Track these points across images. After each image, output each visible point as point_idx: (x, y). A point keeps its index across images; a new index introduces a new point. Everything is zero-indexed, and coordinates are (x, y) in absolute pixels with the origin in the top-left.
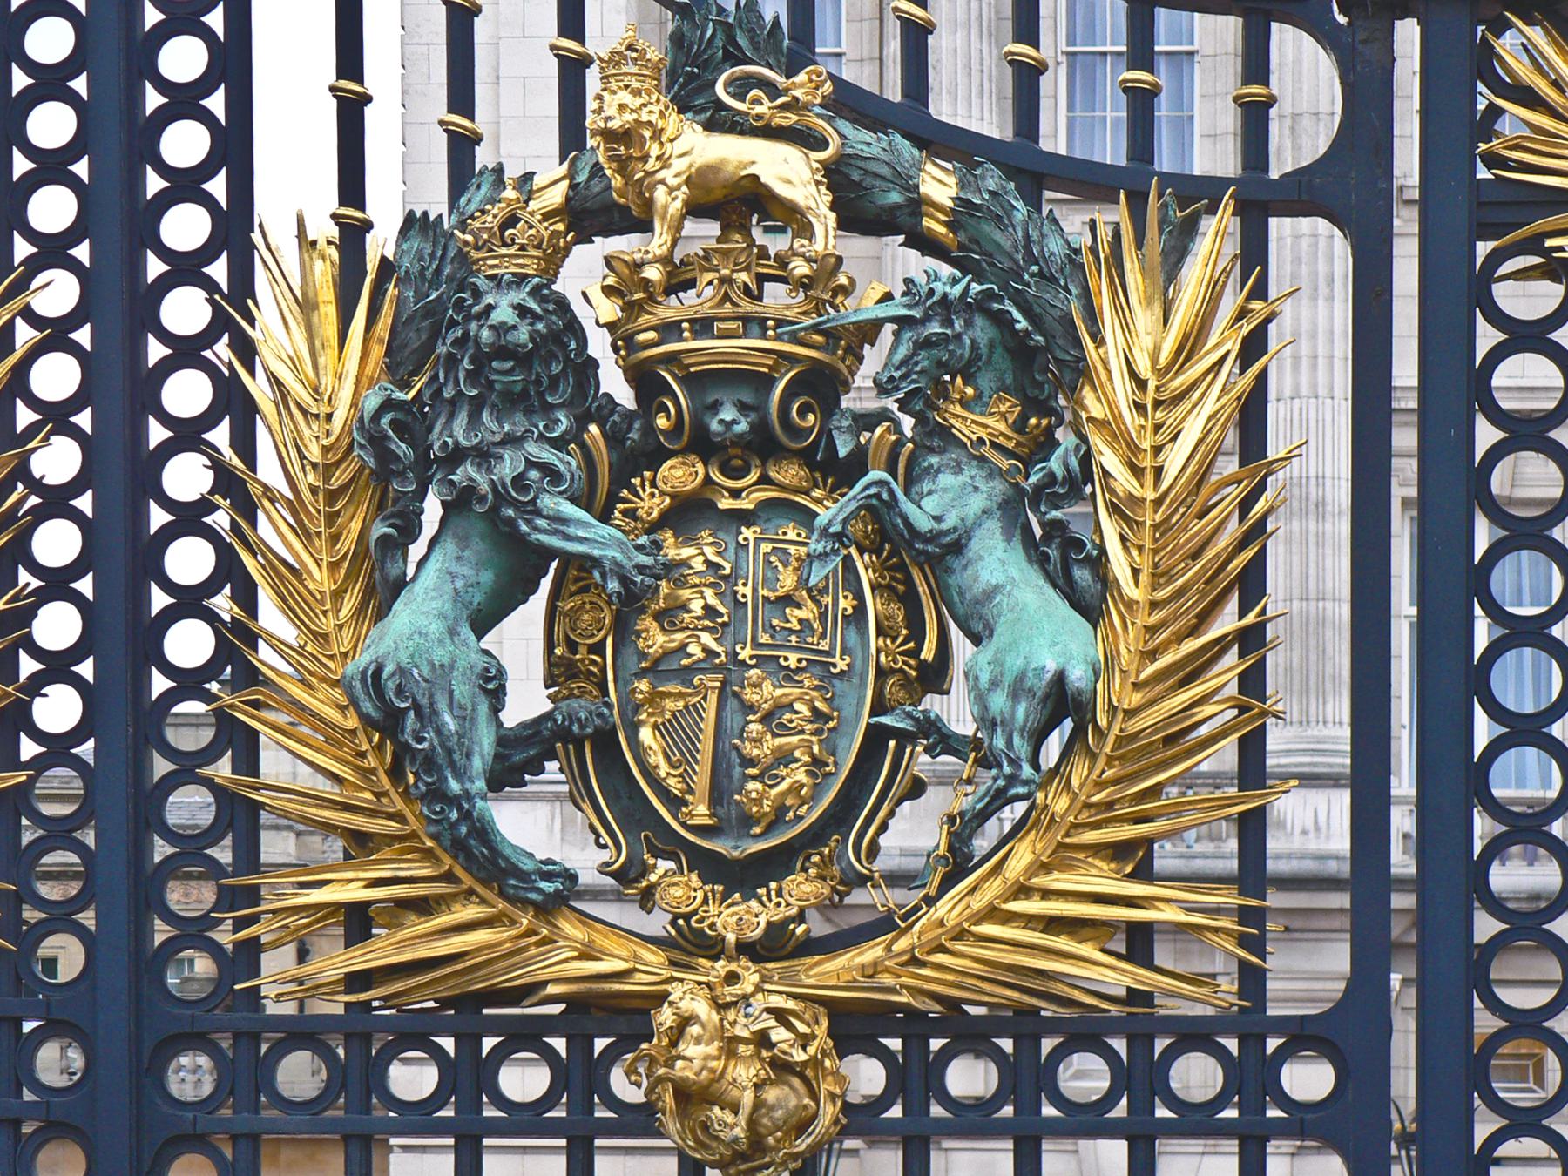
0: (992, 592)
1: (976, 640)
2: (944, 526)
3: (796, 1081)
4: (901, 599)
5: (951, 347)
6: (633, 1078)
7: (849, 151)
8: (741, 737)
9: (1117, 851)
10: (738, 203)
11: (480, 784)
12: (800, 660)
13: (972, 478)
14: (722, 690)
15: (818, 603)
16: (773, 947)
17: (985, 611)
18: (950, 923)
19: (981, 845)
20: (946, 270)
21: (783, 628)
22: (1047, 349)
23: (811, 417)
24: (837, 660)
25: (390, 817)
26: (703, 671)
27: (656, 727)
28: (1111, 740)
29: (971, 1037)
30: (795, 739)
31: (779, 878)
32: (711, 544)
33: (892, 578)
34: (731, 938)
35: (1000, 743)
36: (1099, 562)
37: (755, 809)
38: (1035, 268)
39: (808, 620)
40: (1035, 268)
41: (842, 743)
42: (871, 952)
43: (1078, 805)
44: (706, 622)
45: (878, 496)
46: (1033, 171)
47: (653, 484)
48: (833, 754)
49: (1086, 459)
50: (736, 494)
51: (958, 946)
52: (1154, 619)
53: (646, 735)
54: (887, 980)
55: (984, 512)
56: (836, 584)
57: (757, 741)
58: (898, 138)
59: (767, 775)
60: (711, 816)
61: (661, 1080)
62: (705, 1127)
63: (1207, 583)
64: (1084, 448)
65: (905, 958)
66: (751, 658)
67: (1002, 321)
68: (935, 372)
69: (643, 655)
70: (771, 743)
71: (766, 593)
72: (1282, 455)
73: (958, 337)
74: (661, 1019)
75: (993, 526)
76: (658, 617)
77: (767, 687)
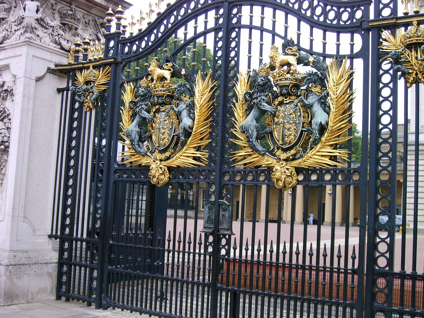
0: (316, 111)
9: (331, 145)
11: (254, 140)
42: (300, 160)
46: (325, 56)
50: (286, 101)
51: (310, 159)
53: (275, 132)
54: (302, 164)
57: (287, 133)
70: (288, 133)
75: (317, 103)
76: (277, 117)
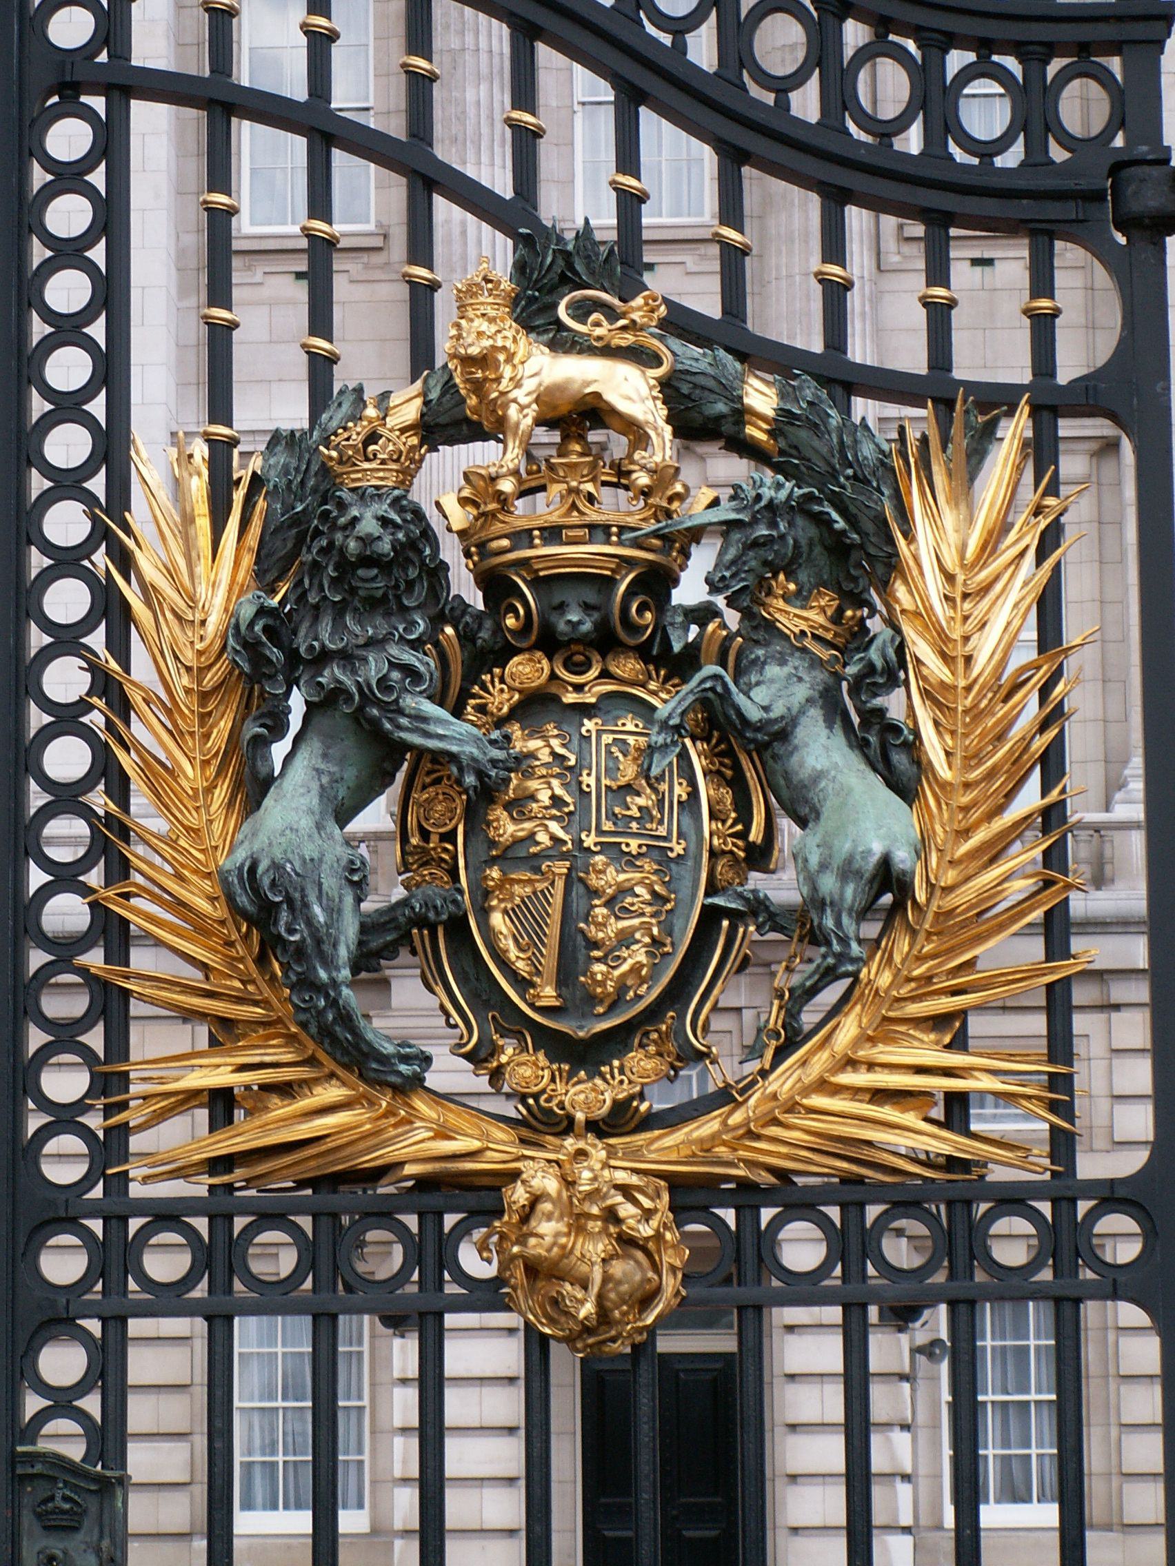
0: (818, 776)
1: (803, 823)
2: (772, 715)
3: (639, 1255)
4: (729, 783)
5: (776, 548)
6: (485, 1255)
7: (680, 367)
8: (586, 922)
10: (580, 416)
12: (640, 846)
13: (796, 668)
14: (568, 876)
15: (655, 790)
16: (618, 1121)
17: (811, 795)
18: (783, 1097)
19: (809, 1018)
20: (768, 476)
21: (624, 816)
22: (861, 547)
23: (648, 615)
24: (673, 844)
25: (256, 1003)
26: (549, 857)
27: (505, 912)
28: (930, 916)
29: (801, 1205)
30: (636, 922)
31: (621, 1054)
32: (556, 736)
33: (721, 764)
34: (580, 1116)
35: (829, 922)
36: (914, 746)
37: (599, 990)
38: (850, 472)
39: (647, 808)
40: (850, 472)
41: (678, 924)
42: (708, 1126)
43: (900, 979)
44: (554, 812)
45: (712, 689)
47: (502, 681)
48: (670, 935)
49: (901, 649)
50: (579, 688)
52: (965, 800)
53: (497, 920)
55: (807, 701)
56: (671, 772)
58: (721, 353)
60: (559, 996)
61: (514, 1258)
62: (555, 1302)
63: (1013, 764)
64: (898, 640)
65: (741, 1132)
66: (596, 844)
67: (822, 521)
68: (760, 570)
69: (493, 844)
70: (615, 926)
71: (608, 783)
72: (1078, 641)
73: (782, 537)
74: (515, 1198)
76: (508, 806)
77: (611, 870)
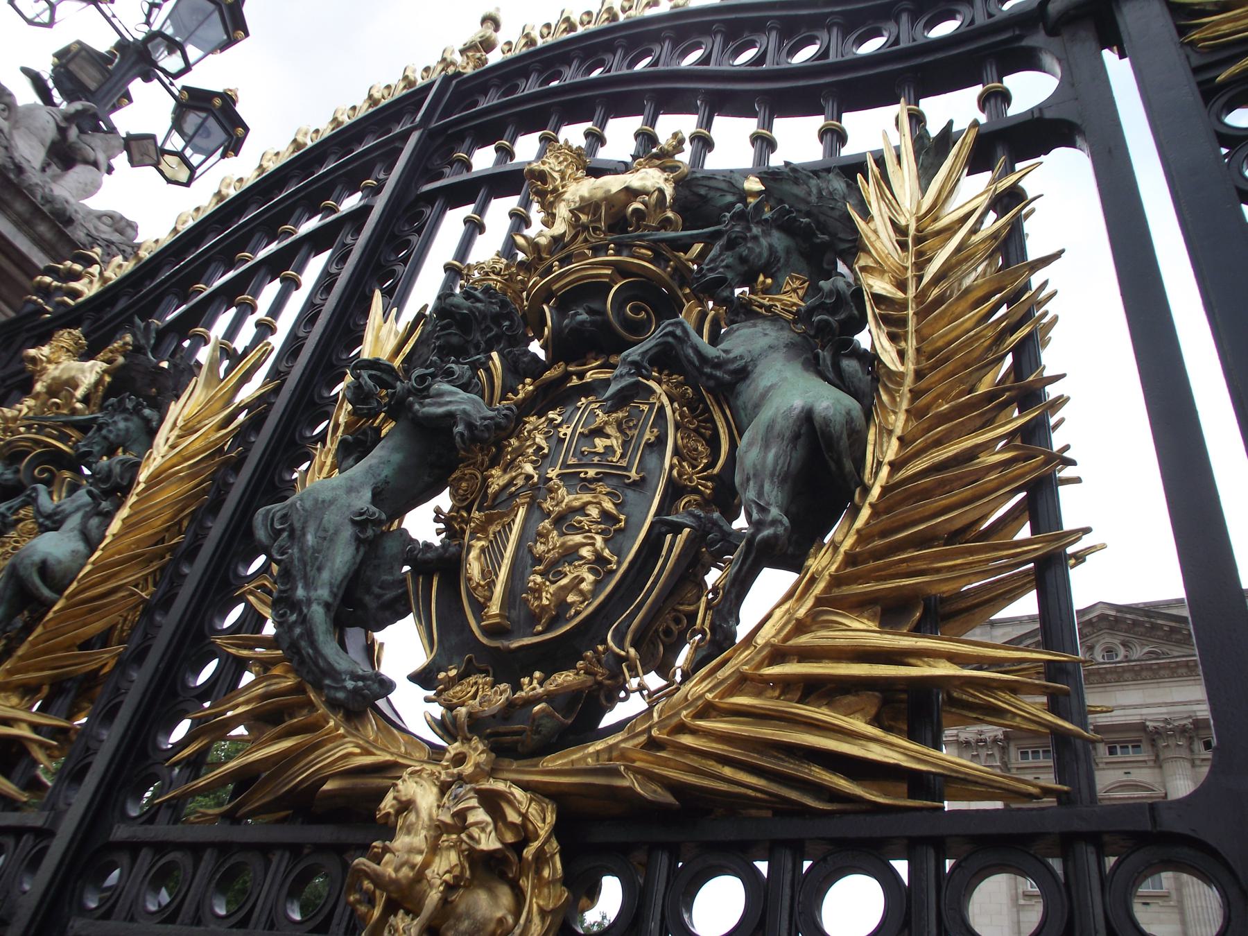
2: (731, 355)
5: (749, 245)
21: (590, 453)
28: (876, 492)
59: (552, 570)
65: (643, 739)
